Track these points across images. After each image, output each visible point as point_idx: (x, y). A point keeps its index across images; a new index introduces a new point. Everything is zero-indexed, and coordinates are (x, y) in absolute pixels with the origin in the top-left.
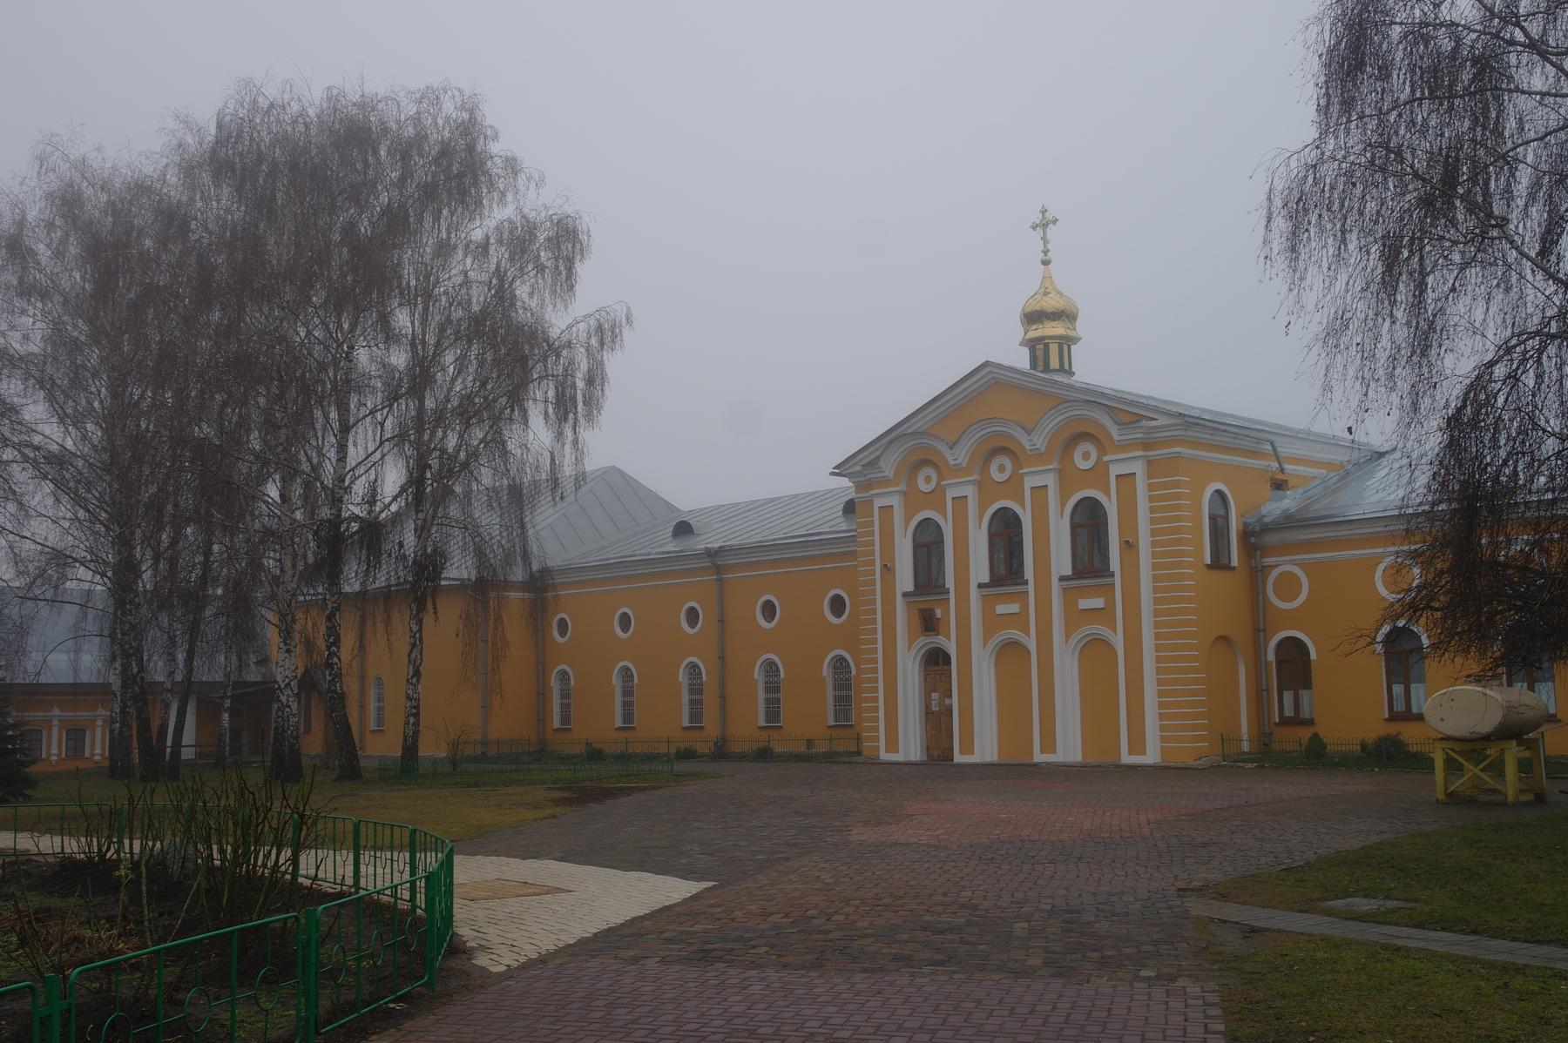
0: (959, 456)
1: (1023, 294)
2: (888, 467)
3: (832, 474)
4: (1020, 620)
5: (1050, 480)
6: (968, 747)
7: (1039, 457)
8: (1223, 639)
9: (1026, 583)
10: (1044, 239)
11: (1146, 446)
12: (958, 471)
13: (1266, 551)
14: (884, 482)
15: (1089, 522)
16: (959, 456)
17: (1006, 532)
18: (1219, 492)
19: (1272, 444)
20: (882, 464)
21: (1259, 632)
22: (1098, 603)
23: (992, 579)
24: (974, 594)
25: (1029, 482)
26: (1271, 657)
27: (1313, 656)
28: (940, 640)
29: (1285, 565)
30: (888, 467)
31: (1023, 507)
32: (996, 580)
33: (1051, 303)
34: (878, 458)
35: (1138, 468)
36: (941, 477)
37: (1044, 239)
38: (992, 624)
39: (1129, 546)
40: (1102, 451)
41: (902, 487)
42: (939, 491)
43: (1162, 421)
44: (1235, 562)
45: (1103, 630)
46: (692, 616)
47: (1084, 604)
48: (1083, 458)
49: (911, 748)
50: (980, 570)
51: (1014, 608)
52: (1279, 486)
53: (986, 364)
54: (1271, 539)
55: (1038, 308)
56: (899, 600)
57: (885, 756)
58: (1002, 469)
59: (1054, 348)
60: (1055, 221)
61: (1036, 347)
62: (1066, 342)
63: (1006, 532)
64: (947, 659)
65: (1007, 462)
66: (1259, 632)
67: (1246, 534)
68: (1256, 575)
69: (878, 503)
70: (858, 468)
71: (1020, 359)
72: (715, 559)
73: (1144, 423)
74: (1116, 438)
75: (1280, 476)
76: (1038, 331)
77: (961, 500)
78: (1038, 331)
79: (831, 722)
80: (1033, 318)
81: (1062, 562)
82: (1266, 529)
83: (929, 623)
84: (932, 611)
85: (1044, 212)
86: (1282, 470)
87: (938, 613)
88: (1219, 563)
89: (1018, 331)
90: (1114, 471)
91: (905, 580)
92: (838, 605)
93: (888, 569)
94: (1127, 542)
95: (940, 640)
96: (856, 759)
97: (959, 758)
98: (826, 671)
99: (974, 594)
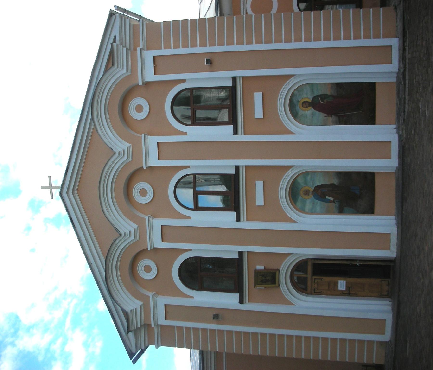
2: (132, 304)
3: (134, 362)
7: (136, 149)
12: (141, 231)
16: (126, 227)
20: (128, 309)
28: (285, 269)
30: (132, 304)
34: (126, 314)
43: (116, 31)
47: (258, 113)
49: (377, 309)
56: (247, 306)
65: (141, 185)
69: (162, 321)
84: (257, 273)
91: (228, 300)
93: (217, 315)
95: (285, 269)
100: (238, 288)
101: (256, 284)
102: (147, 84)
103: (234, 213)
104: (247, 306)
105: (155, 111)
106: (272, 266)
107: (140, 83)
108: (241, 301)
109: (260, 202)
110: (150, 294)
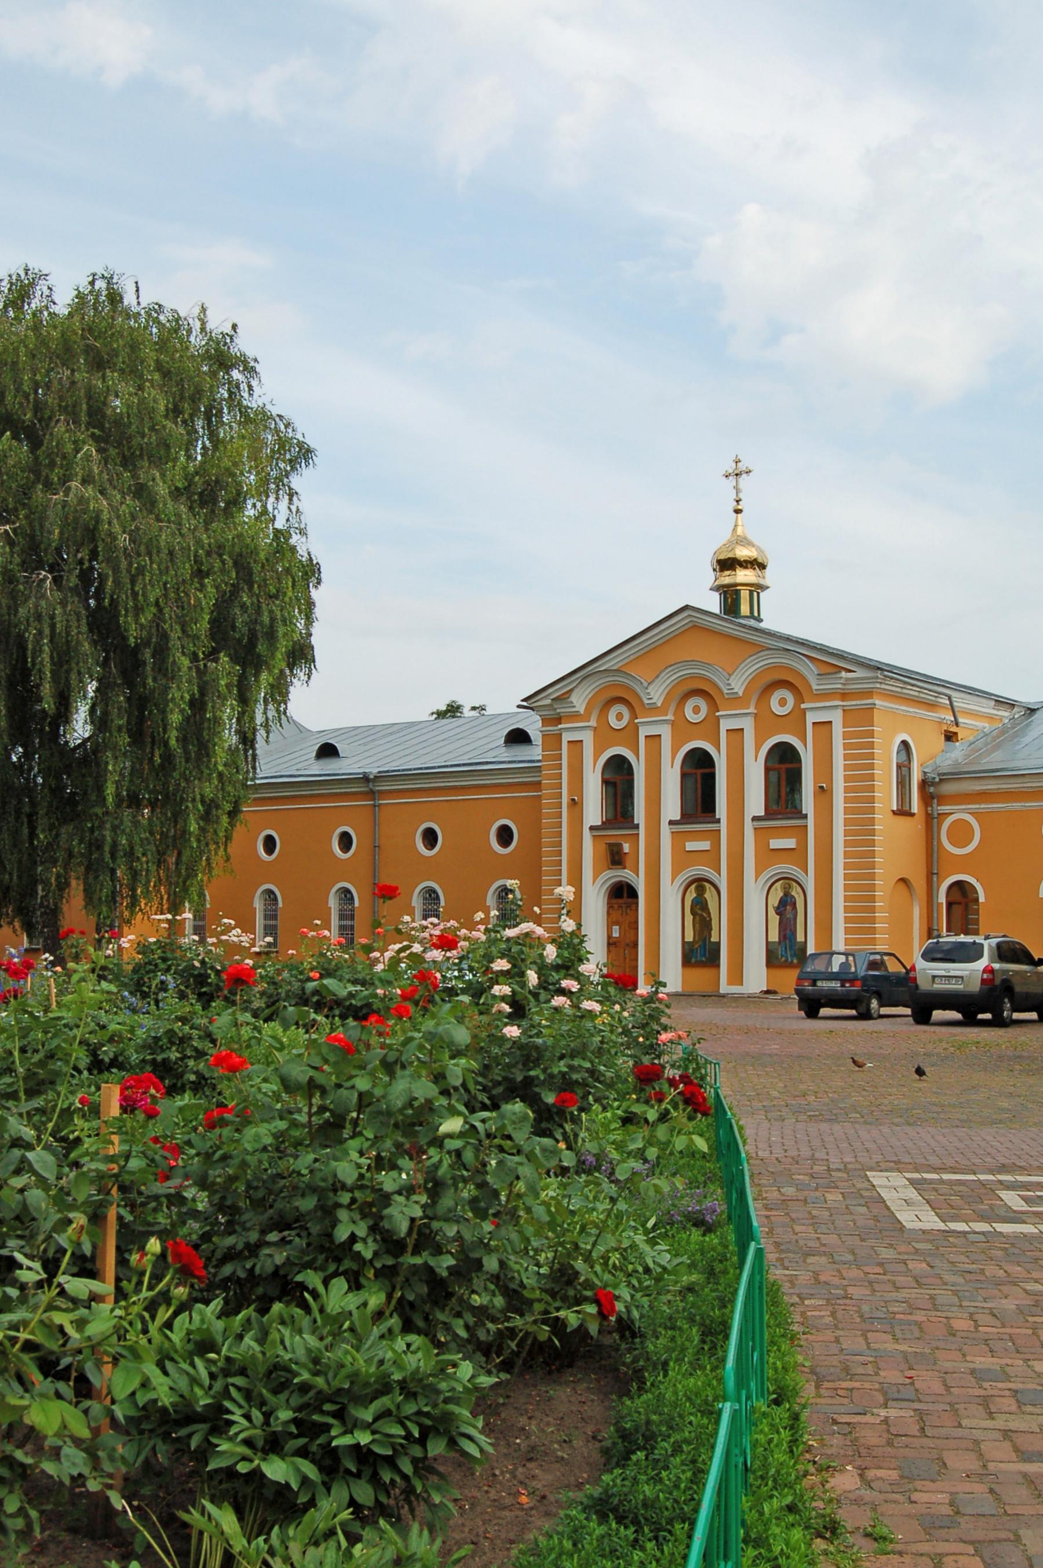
0: (656, 693)
1: (714, 541)
2: (579, 701)
3: (519, 706)
4: (712, 857)
5: (747, 724)
8: (903, 880)
9: (718, 821)
10: (737, 490)
11: (844, 696)
13: (942, 799)
14: (575, 716)
15: (784, 764)
16: (656, 693)
17: (699, 769)
18: (904, 743)
19: (950, 698)
20: (574, 698)
21: (931, 876)
22: (790, 843)
23: (683, 815)
24: (666, 831)
25: (725, 725)
26: (942, 899)
27: (982, 899)
29: (958, 814)
30: (579, 701)
31: (718, 748)
32: (687, 817)
33: (743, 553)
35: (836, 717)
36: (634, 715)
37: (737, 490)
38: (683, 860)
39: (824, 792)
40: (799, 698)
41: (593, 723)
42: (633, 729)
44: (915, 809)
45: (795, 871)
46: (346, 841)
47: (775, 843)
48: (781, 703)
50: (672, 807)
51: (705, 845)
52: (950, 737)
53: (686, 608)
54: (948, 788)
55: (730, 555)
56: (587, 835)
58: (696, 710)
59: (744, 594)
60: (748, 472)
61: (730, 596)
62: (757, 588)
63: (699, 769)
64: (633, 893)
66: (931, 876)
67: (924, 784)
68: (931, 822)
69: (566, 737)
70: (548, 702)
71: (713, 603)
72: (368, 786)
73: (843, 674)
74: (815, 687)
75: (954, 729)
76: (727, 579)
77: (654, 739)
78: (727, 579)
80: (726, 564)
81: (755, 802)
82: (945, 778)
83: (616, 857)
84: (620, 845)
86: (957, 724)
87: (626, 847)
88: (903, 812)
89: (709, 577)
90: (811, 718)
91: (594, 812)
92: (505, 836)
93: (576, 804)
94: (821, 787)
95: (626, 874)
99: (666, 831)
100: (606, 825)
101: (610, 845)
102: (804, 712)
103: (678, 818)
104: (587, 835)
105: (780, 722)
106: (629, 862)
107: (803, 706)
108: (592, 828)
109: (690, 846)
110: (593, 723)
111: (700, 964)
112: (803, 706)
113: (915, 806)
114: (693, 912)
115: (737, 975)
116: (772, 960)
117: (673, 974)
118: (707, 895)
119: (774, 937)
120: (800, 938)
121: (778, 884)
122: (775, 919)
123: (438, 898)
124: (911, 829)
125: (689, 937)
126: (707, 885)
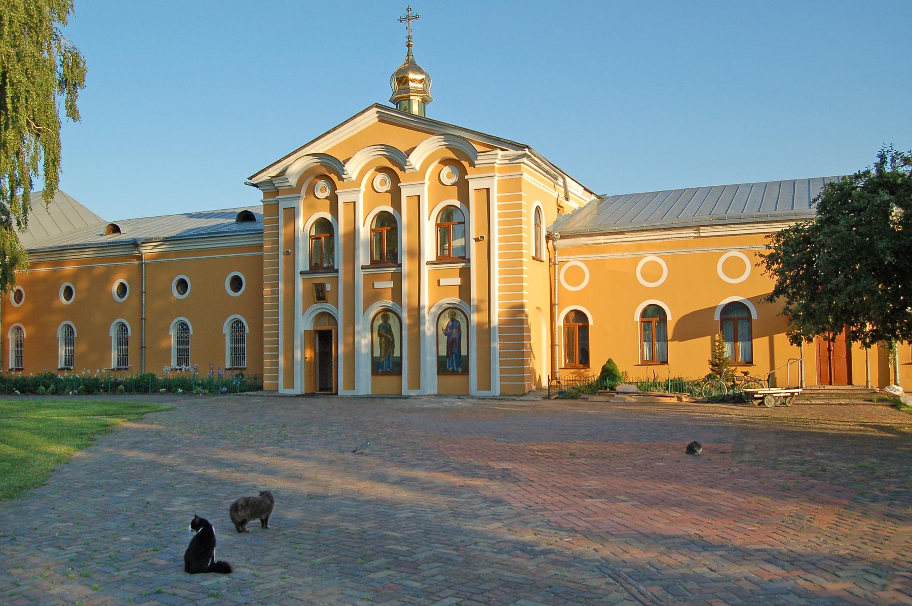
3: (245, 183)
6: (351, 383)
19: (564, 179)
24: (360, 275)
28: (327, 307)
57: (282, 390)
60: (417, 17)
79: (228, 365)
83: (320, 294)
85: (409, 10)
86: (567, 199)
87: (328, 287)
91: (302, 262)
92: (236, 283)
95: (327, 307)
96: (260, 393)
97: (341, 391)
98: (227, 330)
100: (315, 268)
101: (316, 285)
102: (467, 182)
106: (329, 297)
107: (466, 177)
108: (302, 273)
111: (385, 373)
112: (466, 177)
113: (545, 256)
114: (380, 335)
115: (416, 382)
116: (443, 368)
117: (365, 383)
118: (391, 322)
119: (443, 352)
120: (464, 352)
121: (446, 313)
122: (444, 340)
123: (188, 329)
124: (543, 269)
125: (377, 354)
126: (391, 314)
